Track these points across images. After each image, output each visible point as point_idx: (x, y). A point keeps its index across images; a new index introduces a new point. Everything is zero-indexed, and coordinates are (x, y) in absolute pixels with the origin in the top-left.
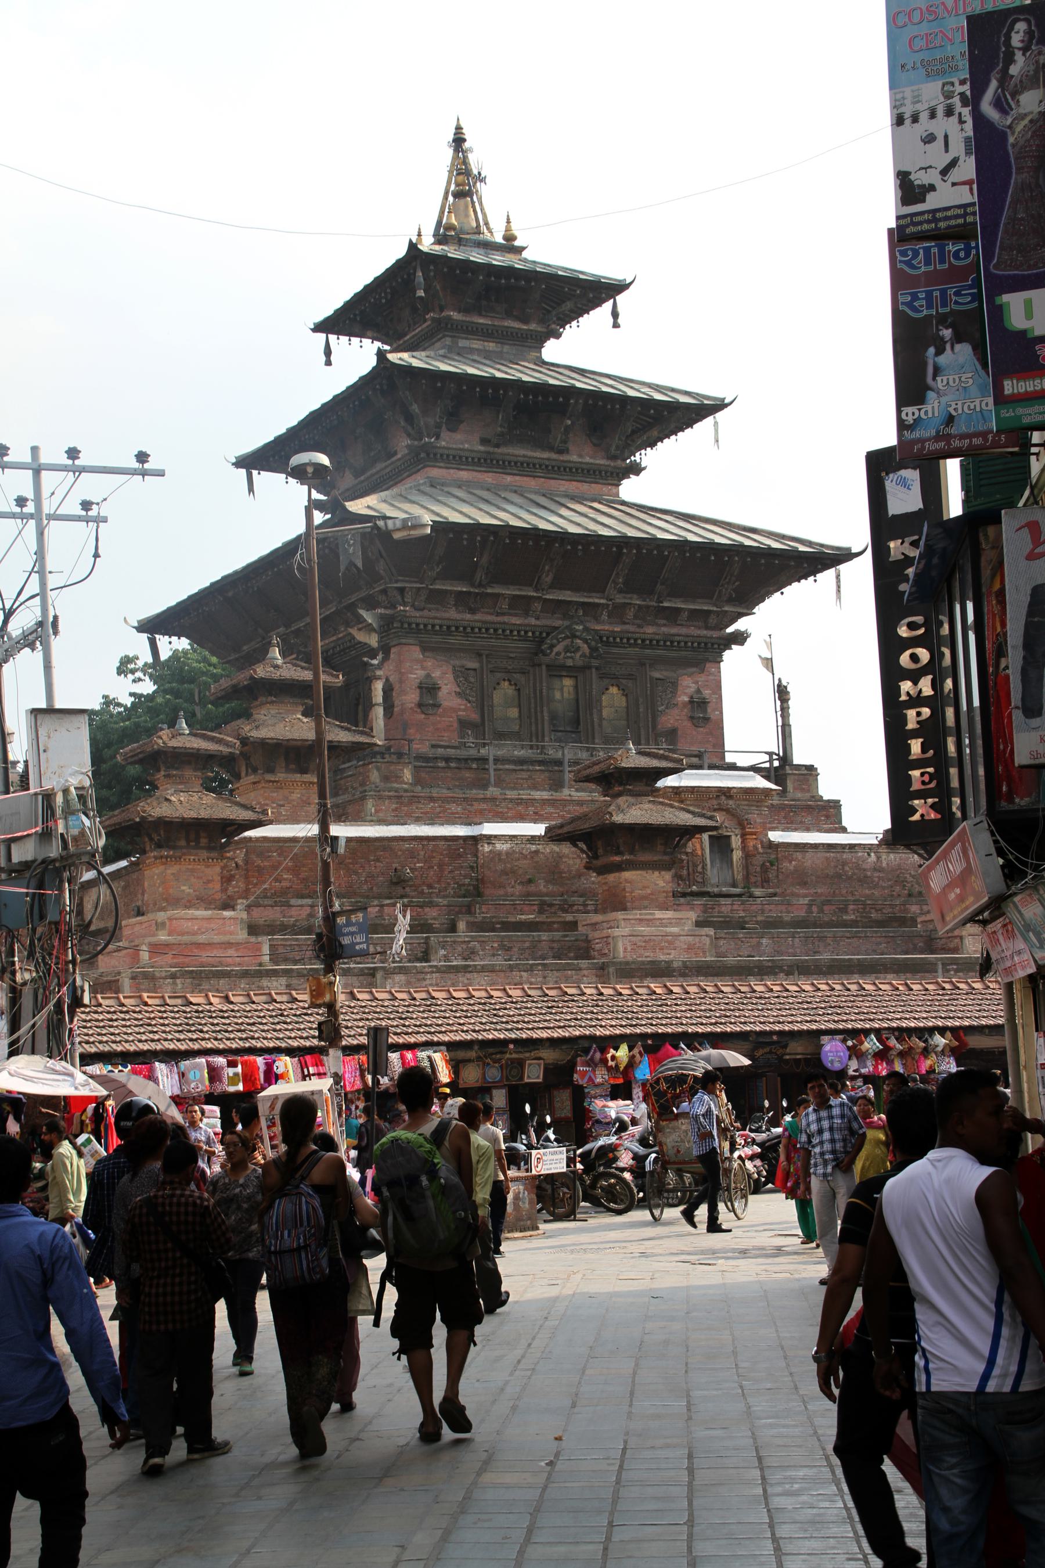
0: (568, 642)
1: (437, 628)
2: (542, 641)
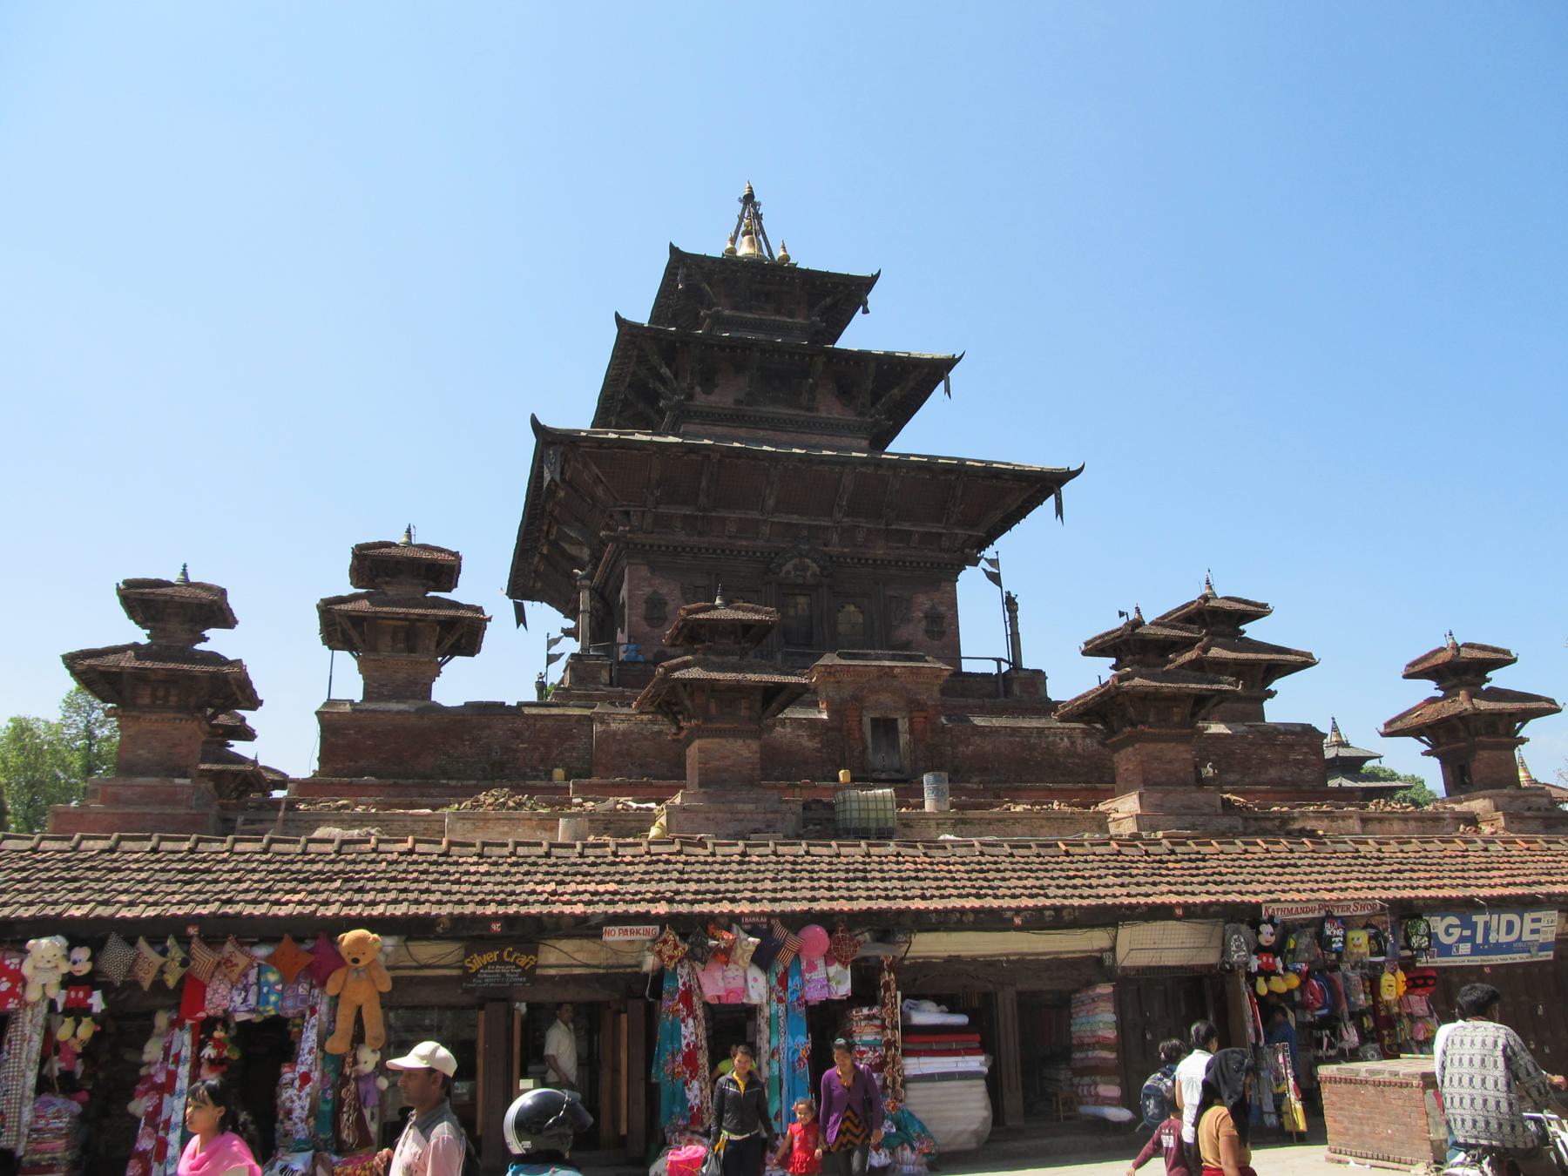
0: (796, 561)
1: (663, 548)
2: (773, 558)
